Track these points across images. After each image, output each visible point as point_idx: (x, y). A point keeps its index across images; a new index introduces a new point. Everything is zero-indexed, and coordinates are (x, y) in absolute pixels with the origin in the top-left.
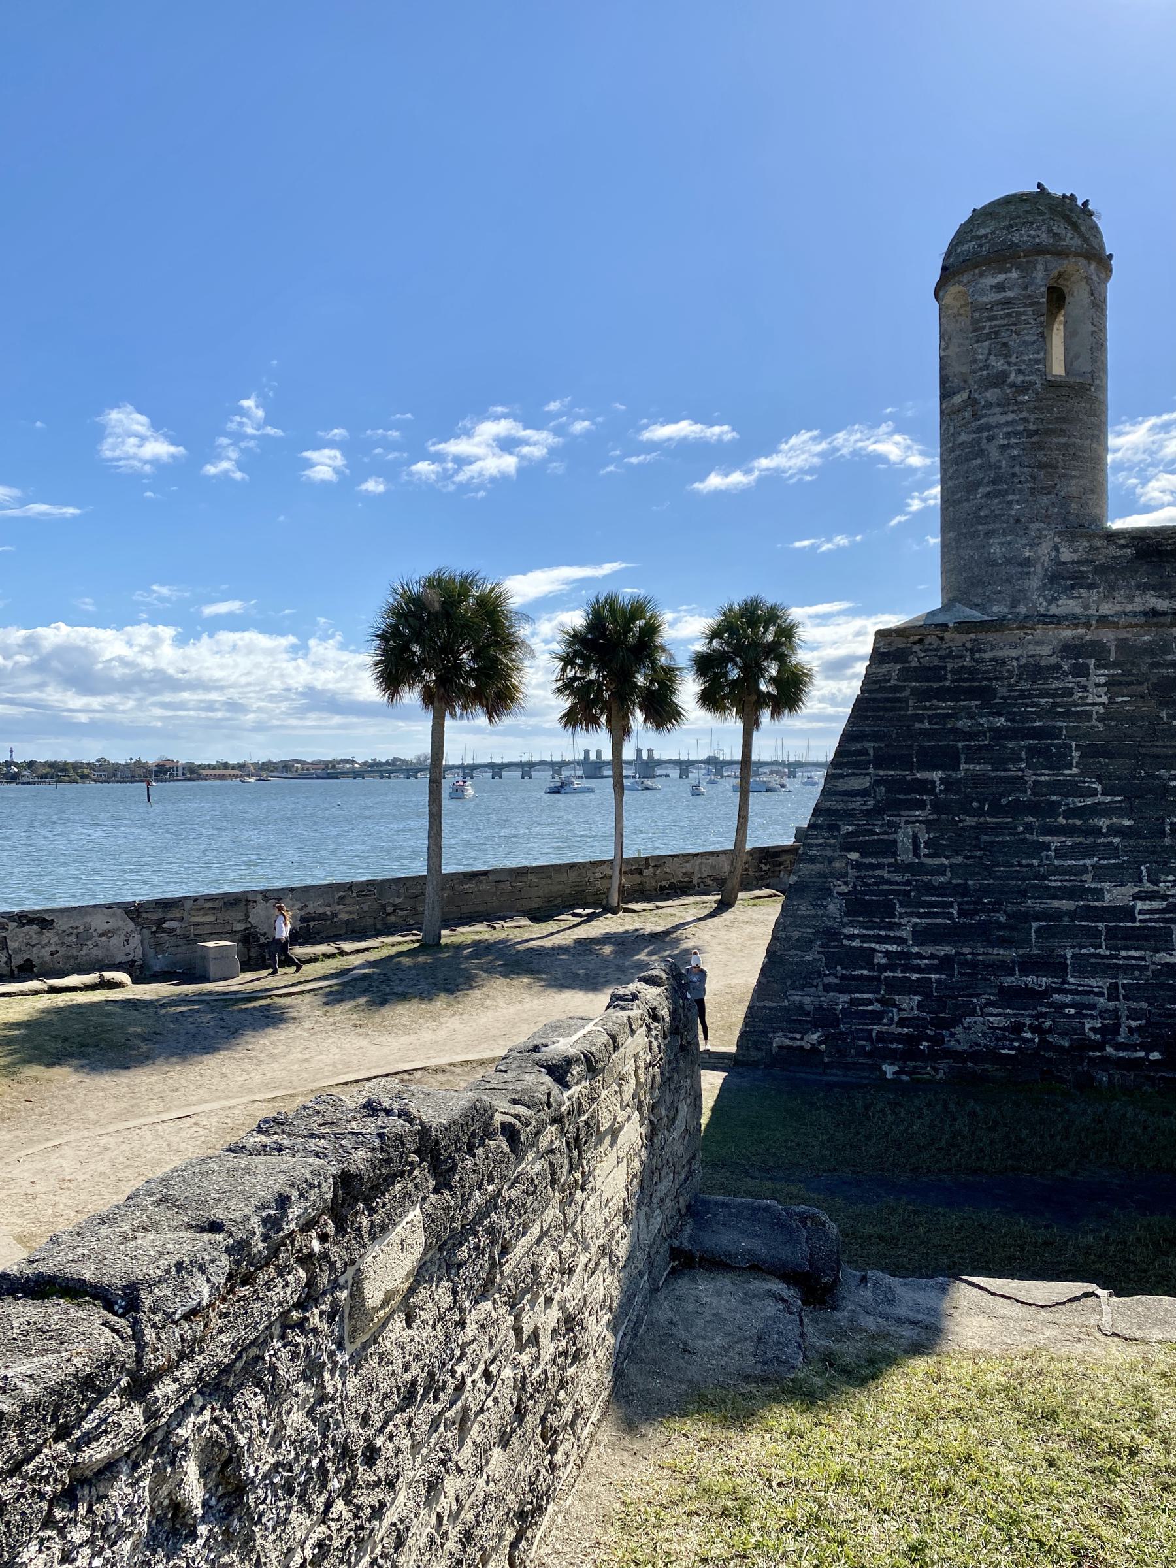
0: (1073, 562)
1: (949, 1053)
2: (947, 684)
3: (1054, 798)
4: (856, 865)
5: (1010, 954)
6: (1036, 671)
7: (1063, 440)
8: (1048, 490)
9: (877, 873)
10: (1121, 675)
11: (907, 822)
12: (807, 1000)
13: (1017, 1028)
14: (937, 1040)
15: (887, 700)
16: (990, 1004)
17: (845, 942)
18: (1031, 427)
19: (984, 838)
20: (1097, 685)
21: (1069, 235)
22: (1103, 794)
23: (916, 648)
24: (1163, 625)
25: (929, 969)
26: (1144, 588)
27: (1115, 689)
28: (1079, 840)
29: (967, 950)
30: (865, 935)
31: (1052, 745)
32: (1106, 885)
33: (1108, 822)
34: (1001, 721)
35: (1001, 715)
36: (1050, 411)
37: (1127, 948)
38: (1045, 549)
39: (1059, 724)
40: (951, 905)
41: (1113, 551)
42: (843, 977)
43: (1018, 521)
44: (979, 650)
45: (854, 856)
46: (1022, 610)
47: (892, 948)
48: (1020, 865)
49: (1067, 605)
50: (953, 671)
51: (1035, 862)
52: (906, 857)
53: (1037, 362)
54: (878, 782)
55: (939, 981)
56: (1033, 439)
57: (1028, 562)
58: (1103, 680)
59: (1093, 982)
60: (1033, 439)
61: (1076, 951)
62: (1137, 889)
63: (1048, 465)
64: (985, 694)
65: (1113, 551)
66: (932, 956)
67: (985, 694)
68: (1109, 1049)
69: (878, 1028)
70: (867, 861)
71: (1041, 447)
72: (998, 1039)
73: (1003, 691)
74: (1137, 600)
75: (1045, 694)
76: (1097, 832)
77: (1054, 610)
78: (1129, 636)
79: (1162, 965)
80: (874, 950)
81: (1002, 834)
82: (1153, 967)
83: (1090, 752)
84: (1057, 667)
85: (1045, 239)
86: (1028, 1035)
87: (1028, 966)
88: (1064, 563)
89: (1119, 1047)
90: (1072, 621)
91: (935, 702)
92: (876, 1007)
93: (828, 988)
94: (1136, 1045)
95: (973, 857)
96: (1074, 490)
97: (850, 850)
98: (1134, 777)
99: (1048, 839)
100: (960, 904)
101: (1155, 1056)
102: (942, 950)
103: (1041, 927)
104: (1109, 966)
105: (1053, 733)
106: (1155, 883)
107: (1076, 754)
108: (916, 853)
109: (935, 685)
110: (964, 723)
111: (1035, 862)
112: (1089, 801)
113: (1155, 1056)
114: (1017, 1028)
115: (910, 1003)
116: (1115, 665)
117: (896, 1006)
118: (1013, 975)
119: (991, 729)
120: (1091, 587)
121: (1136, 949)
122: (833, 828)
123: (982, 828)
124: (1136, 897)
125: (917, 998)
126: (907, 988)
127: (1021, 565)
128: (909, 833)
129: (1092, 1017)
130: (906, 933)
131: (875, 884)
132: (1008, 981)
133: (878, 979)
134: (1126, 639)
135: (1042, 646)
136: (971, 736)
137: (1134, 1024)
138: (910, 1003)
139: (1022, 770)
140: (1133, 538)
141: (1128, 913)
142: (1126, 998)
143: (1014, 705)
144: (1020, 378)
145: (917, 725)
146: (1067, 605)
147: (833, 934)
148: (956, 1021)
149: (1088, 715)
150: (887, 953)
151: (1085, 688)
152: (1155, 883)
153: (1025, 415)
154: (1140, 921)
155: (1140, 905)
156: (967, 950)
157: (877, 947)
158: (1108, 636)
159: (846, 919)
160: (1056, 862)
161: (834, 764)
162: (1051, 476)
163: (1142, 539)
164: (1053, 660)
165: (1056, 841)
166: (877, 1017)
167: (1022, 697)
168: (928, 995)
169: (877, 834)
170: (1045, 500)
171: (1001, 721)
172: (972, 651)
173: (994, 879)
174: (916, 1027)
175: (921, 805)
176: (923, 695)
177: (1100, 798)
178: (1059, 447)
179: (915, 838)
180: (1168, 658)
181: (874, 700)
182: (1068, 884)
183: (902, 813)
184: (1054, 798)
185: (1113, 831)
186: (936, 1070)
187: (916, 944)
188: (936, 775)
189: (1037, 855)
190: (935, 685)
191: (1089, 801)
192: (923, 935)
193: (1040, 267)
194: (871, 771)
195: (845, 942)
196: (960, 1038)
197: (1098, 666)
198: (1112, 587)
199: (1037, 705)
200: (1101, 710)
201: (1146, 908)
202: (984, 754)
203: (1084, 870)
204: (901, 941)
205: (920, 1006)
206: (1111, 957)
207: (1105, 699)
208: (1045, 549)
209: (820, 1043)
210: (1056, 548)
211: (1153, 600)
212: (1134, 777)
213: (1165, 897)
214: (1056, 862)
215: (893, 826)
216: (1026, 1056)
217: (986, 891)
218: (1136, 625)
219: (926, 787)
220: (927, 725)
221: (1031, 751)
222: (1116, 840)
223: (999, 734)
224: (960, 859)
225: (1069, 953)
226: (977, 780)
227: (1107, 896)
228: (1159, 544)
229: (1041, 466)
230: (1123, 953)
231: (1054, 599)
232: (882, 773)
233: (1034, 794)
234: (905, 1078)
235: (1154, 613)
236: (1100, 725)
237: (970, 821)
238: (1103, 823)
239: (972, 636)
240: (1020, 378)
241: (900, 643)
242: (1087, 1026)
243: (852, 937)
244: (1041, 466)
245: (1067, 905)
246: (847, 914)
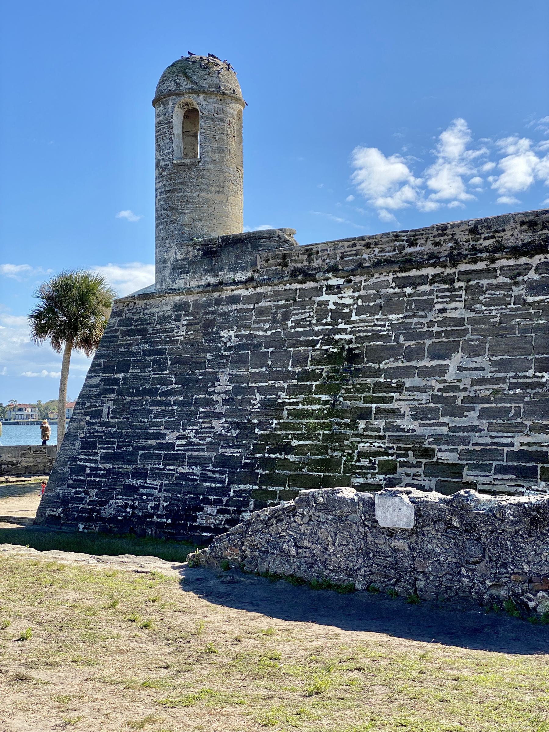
0: (182, 260)
1: (102, 519)
2: (133, 327)
3: (158, 386)
4: (88, 423)
5: (128, 468)
6: (164, 319)
7: (180, 194)
8: (173, 222)
9: (94, 427)
10: (193, 320)
11: (108, 400)
12: (61, 491)
13: (126, 506)
14: (99, 512)
15: (113, 337)
16: (119, 494)
17: (78, 463)
18: (167, 189)
19: (132, 408)
20: (183, 325)
21: (185, 83)
22: (175, 384)
23: (126, 309)
24: (210, 292)
25: (103, 476)
26: (206, 271)
27: (189, 327)
28: (163, 408)
29: (116, 466)
30: (85, 459)
31: (162, 358)
32: (168, 432)
33: (174, 398)
34: (147, 346)
35: (147, 343)
36: (174, 180)
37: (169, 465)
38: (172, 253)
39: (167, 347)
40: (113, 443)
41: (195, 253)
42: (75, 480)
43: (163, 239)
44: (147, 309)
45: (88, 418)
46: (164, 287)
47: (93, 465)
48: (141, 422)
49: (179, 284)
50: (136, 321)
51: (146, 420)
52: (105, 419)
53: (169, 154)
54: (102, 380)
55: (105, 482)
56: (168, 195)
57: (165, 261)
58: (185, 322)
59: (153, 482)
60: (168, 195)
61: (152, 466)
62: (178, 434)
63: (174, 209)
64: (142, 332)
65: (195, 253)
66: (105, 469)
67: (142, 332)
68: (155, 517)
69: (81, 506)
70: (91, 421)
71: (170, 199)
72: (118, 512)
73: (151, 331)
74: (203, 278)
75: (165, 331)
76: (168, 404)
77: (175, 286)
78: (198, 298)
79: (180, 473)
80: (86, 466)
81: (138, 406)
82: (176, 475)
83: (176, 361)
84: (171, 316)
85: (173, 87)
86: (128, 510)
87: (136, 474)
88: (178, 261)
89: (159, 516)
90: (179, 292)
91: (127, 337)
92: (82, 495)
93: (69, 486)
94: (164, 515)
95: (126, 418)
96: (187, 220)
97: (87, 415)
98: (187, 374)
99: (151, 408)
100: (118, 442)
101: (169, 521)
102: (109, 466)
103: (143, 454)
104: (161, 474)
105: (161, 352)
106: (184, 430)
107: (169, 363)
108: (108, 417)
109: (129, 328)
110: (134, 348)
111: (146, 420)
112: (170, 387)
113: (169, 521)
114: (126, 506)
115: (93, 492)
116: (192, 314)
117: (89, 494)
118: (128, 478)
119: (143, 351)
120: (188, 272)
121: (173, 465)
122: (84, 404)
123: (131, 403)
124: (178, 438)
125: (96, 490)
126: (92, 485)
127: (163, 263)
128: (108, 406)
129: (151, 500)
130: (98, 458)
131: (93, 433)
132: (127, 481)
133: (85, 481)
134: (197, 300)
135: (165, 306)
136: (136, 354)
137: (165, 504)
138: (93, 492)
139: (149, 372)
140: (202, 245)
141: (172, 446)
142: (165, 491)
143: (152, 337)
144: (163, 163)
145: (120, 350)
146: (179, 284)
147: (74, 458)
148: (106, 503)
149: (177, 341)
150: (91, 467)
151: (178, 327)
152: (184, 430)
153: (165, 182)
154: (177, 450)
155: (179, 442)
156: (116, 466)
157: (88, 465)
158: (190, 299)
159: (80, 451)
160: (153, 420)
161: (90, 372)
162: (174, 214)
163: (205, 245)
164: (170, 313)
165: (155, 409)
166: (82, 499)
167: (156, 333)
168: (99, 489)
169: (97, 407)
170: (172, 227)
171: (147, 346)
172: (144, 309)
173: (132, 429)
174: (93, 505)
175: (112, 391)
176: (125, 333)
177: (174, 386)
178: (179, 198)
179: (109, 408)
180: (210, 309)
181: (108, 337)
182: (155, 431)
183: (107, 396)
184: (158, 386)
185: (176, 403)
186: (95, 527)
187: (101, 463)
188: (121, 376)
189: (146, 416)
190: (129, 328)
191: (170, 387)
192: (106, 458)
193: (170, 103)
194: (101, 374)
195: (78, 463)
196: (108, 511)
197: (186, 315)
198: (195, 273)
199: (160, 337)
200: (182, 338)
201: (179, 443)
202: (139, 364)
203: (160, 424)
204: (95, 461)
205: (96, 495)
206: (163, 469)
207: (184, 333)
208: (172, 253)
209: (61, 513)
210: (176, 253)
211: (209, 278)
212: (187, 374)
213: (187, 438)
214: (153, 420)
215: (103, 402)
216: (127, 521)
217: (128, 435)
218: (200, 292)
219: (116, 381)
220: (123, 350)
221: (155, 361)
222: (176, 408)
223: (146, 353)
224: (121, 419)
225: (150, 467)
226: (135, 377)
227: (167, 437)
228: (211, 248)
229: (171, 209)
230: (168, 467)
231: (175, 280)
232: (104, 375)
233: (152, 384)
234: (86, 531)
235: (209, 285)
236: (181, 347)
237: (128, 399)
238: (172, 399)
239: (145, 301)
240: (163, 163)
241: (121, 306)
242: (149, 505)
243: (81, 460)
244: (171, 209)
245: (153, 442)
246: (81, 449)
